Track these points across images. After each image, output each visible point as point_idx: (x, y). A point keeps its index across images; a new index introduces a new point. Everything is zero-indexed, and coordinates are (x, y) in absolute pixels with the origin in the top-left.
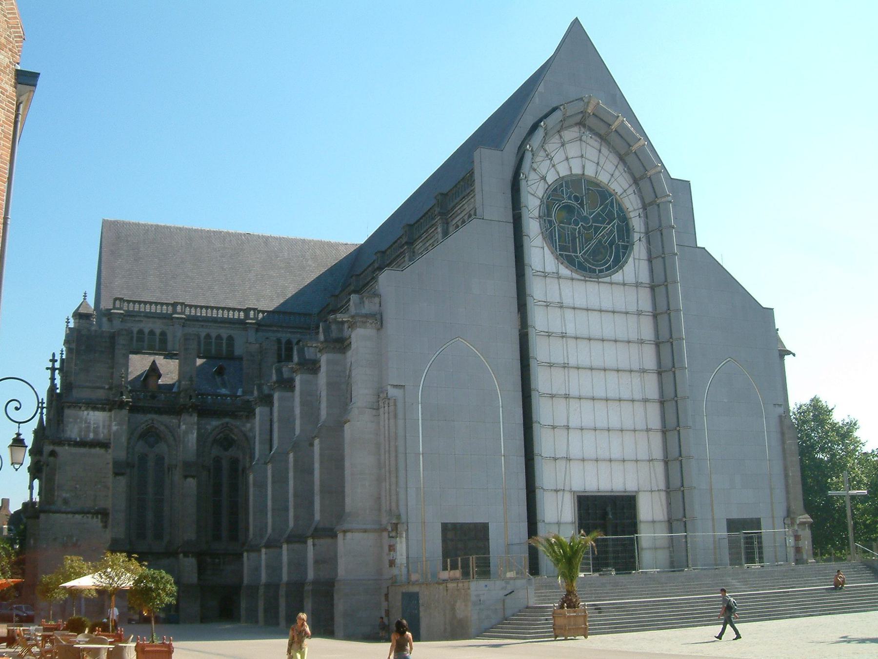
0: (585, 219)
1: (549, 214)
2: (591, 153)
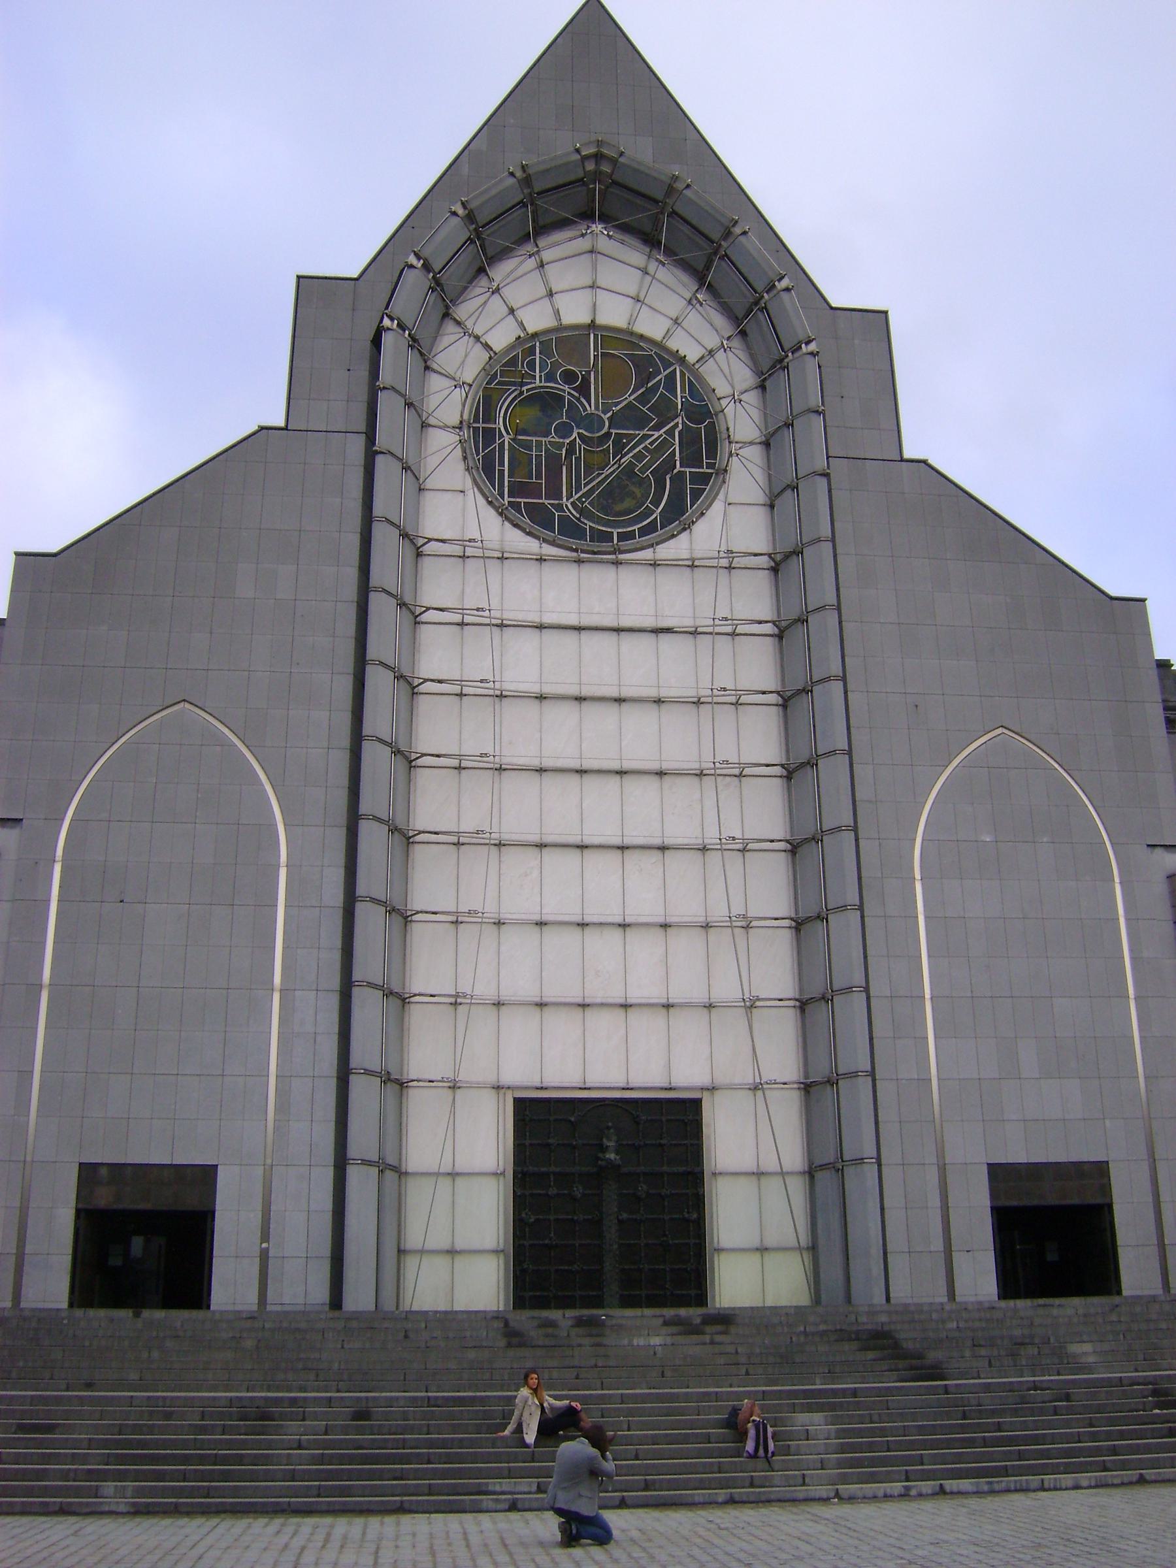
0: (592, 422)
1: (489, 417)
2: (629, 280)
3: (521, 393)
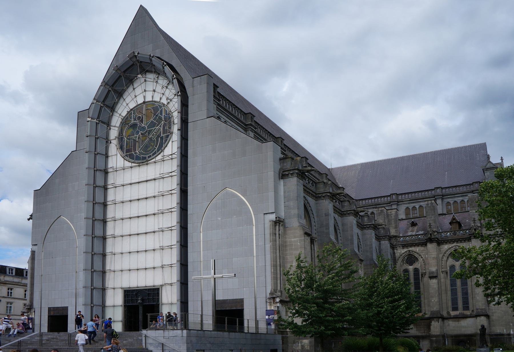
0: (144, 128)
3: (129, 125)
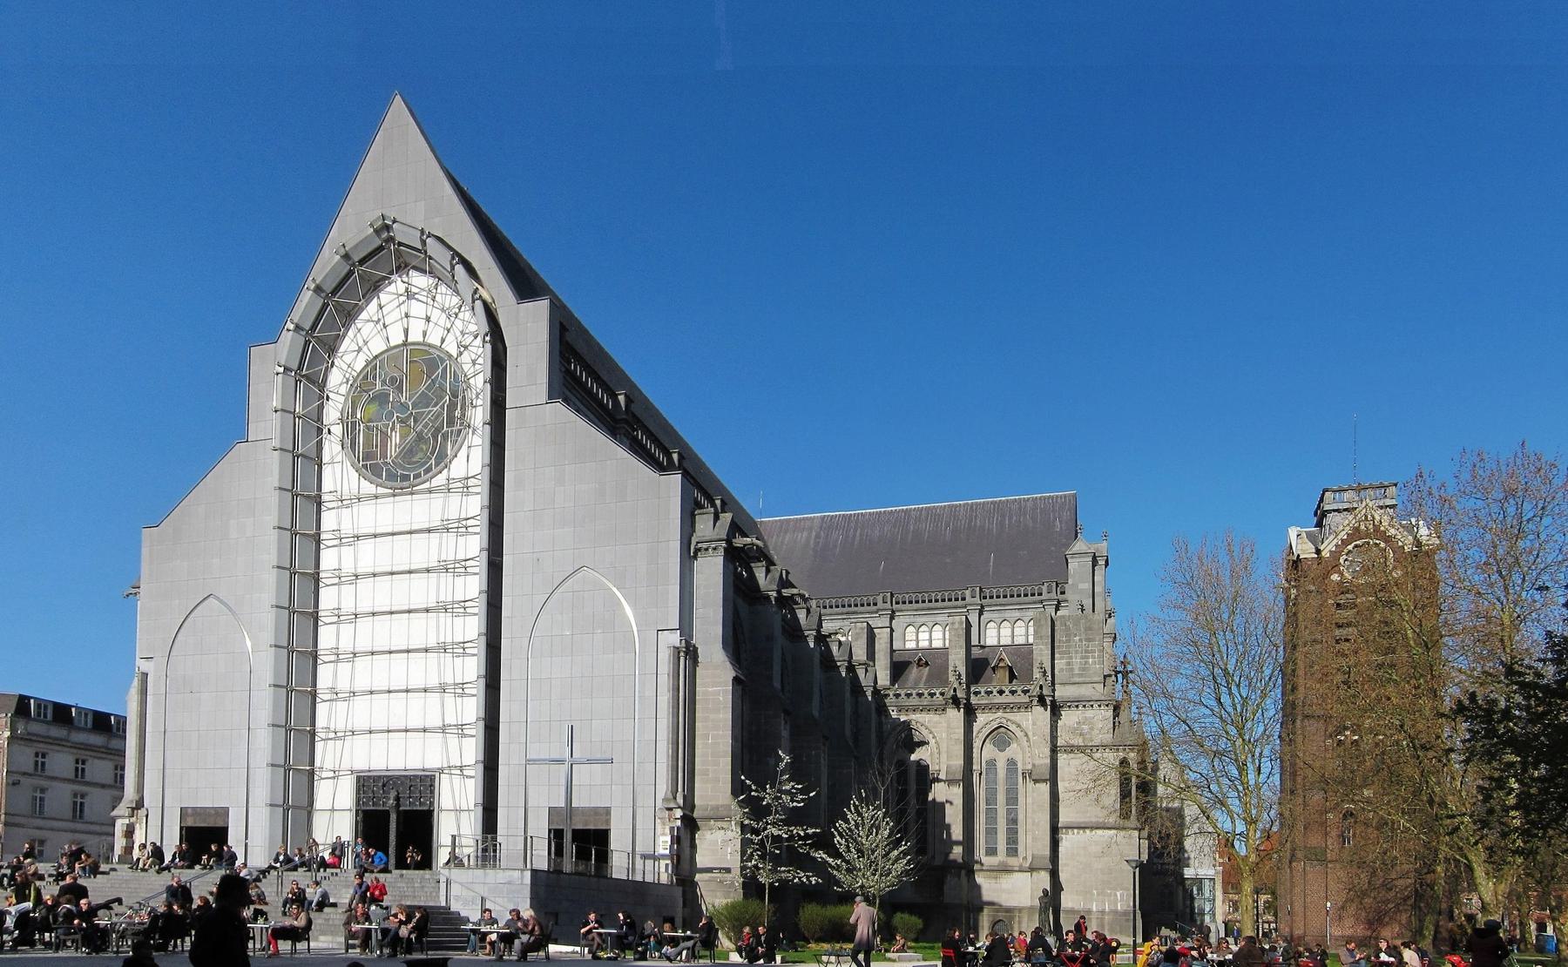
0: (404, 406)
